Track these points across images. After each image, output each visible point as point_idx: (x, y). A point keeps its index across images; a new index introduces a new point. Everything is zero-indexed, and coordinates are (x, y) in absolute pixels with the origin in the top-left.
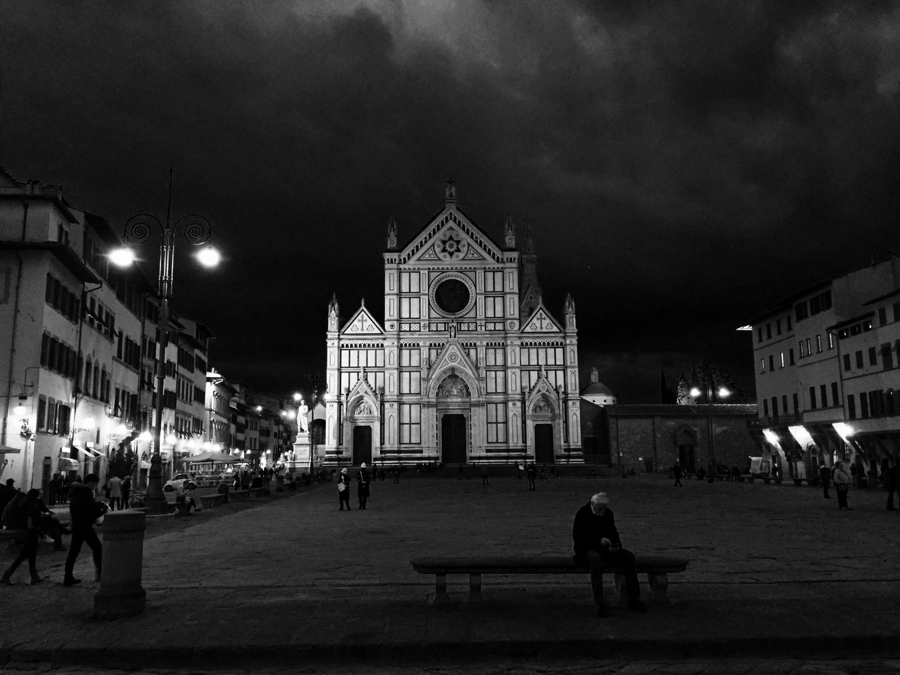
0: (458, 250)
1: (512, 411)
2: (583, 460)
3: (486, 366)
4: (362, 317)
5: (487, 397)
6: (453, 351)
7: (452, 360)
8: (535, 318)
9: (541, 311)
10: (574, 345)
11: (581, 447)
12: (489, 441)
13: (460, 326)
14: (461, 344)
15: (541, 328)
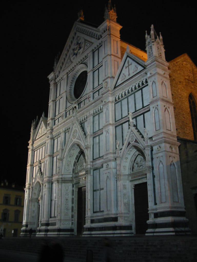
0: (80, 48)
1: (106, 173)
2: (171, 229)
3: (93, 133)
4: (42, 125)
5: (94, 163)
6: (75, 129)
7: (74, 137)
8: (124, 67)
9: (128, 58)
10: (154, 75)
11: (169, 210)
12: (95, 211)
13: (80, 105)
14: (79, 120)
15: (129, 75)
